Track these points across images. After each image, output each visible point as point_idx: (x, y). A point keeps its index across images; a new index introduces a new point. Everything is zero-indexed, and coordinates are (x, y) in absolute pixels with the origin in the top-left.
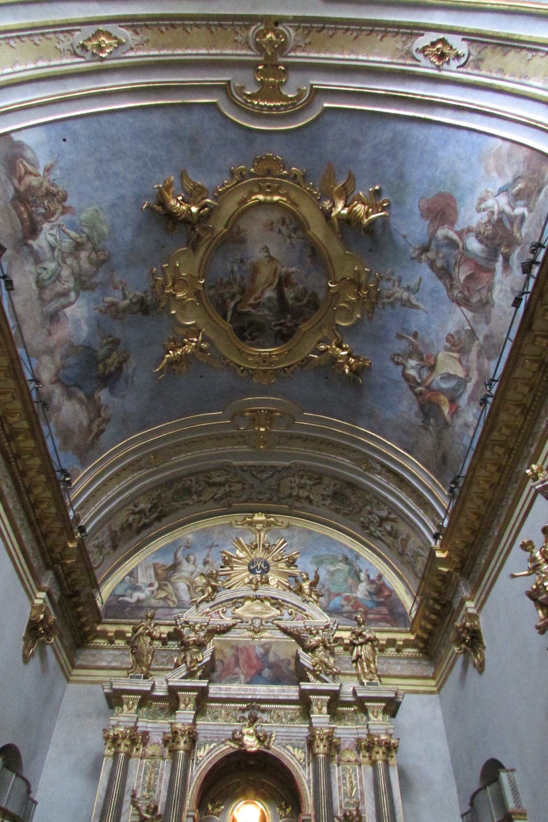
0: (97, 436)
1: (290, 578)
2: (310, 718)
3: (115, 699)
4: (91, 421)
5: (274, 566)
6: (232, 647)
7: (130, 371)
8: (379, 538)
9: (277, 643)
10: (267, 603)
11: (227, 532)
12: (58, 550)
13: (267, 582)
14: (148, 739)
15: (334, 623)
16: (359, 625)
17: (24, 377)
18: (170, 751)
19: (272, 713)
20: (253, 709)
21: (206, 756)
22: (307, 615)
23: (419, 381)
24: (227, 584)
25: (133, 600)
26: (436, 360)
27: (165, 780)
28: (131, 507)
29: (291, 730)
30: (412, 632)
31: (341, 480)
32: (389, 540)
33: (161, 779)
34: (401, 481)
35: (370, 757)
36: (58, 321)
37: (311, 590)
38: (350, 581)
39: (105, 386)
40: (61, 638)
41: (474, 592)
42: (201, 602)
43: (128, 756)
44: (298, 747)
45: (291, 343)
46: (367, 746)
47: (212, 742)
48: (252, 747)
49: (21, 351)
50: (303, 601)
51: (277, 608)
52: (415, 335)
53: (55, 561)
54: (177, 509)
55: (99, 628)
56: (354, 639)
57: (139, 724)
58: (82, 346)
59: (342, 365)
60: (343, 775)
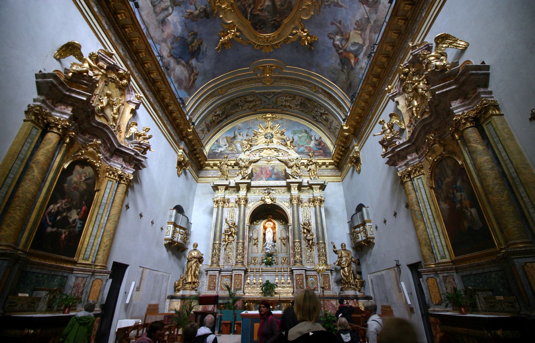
0: (194, 82)
3: (216, 188)
4: (190, 75)
7: (204, 49)
8: (320, 122)
9: (278, 165)
10: (273, 150)
11: (255, 122)
12: (184, 133)
16: (311, 157)
17: (154, 55)
20: (268, 188)
21: (252, 206)
23: (341, 47)
24: (256, 144)
25: (219, 151)
26: (349, 35)
28: (213, 113)
30: (333, 159)
31: (304, 97)
32: (325, 123)
34: (331, 97)
36: (166, 24)
38: (308, 140)
39: (194, 58)
40: (192, 167)
41: (359, 142)
43: (223, 207)
45: (280, 30)
46: (313, 201)
49: (150, 41)
52: (340, 22)
53: (184, 137)
54: (233, 113)
55: (206, 162)
58: (179, 37)
59: (304, 40)
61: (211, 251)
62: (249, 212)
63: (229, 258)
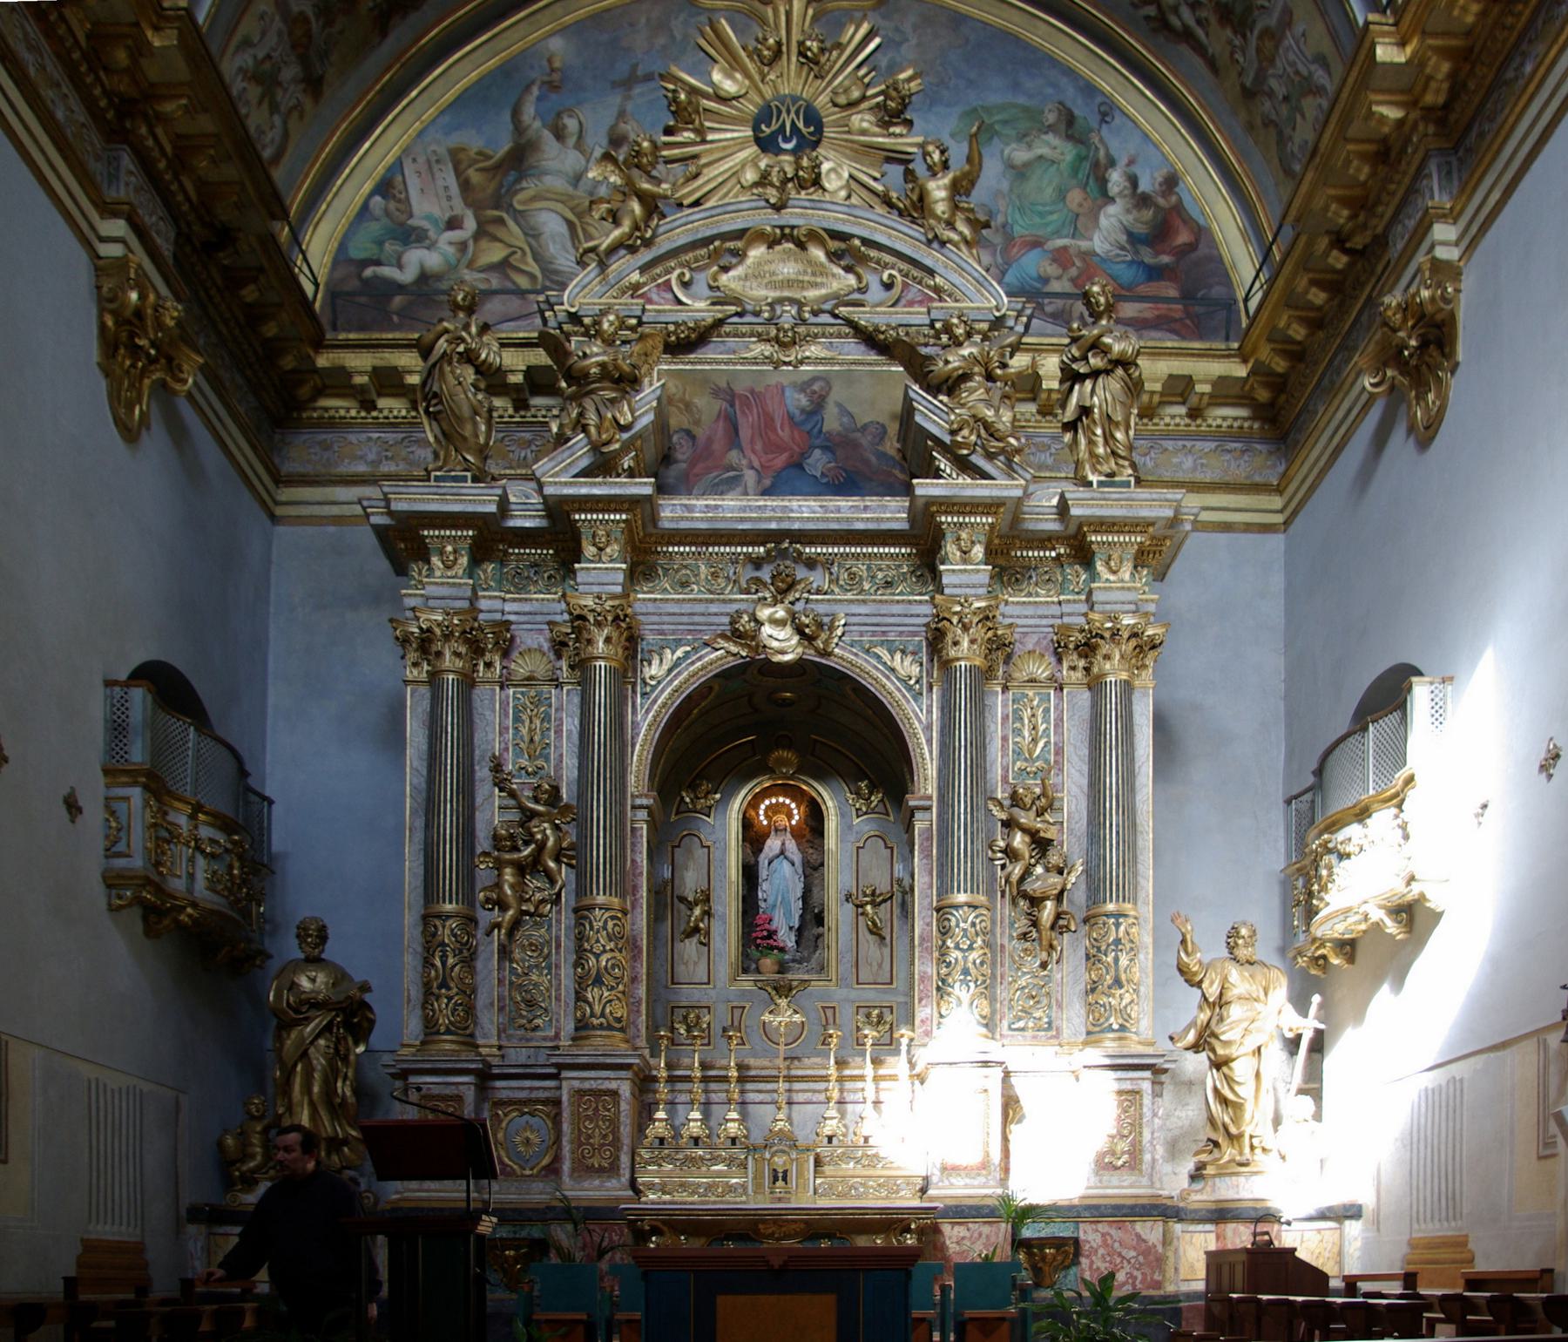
1: (887, 167)
2: (936, 576)
3: (405, 542)
5: (836, 124)
6: (716, 393)
9: (848, 378)
10: (818, 253)
13: (817, 182)
14: (513, 638)
15: (1020, 314)
16: (1096, 316)
18: (572, 667)
19: (835, 569)
20: (780, 556)
21: (669, 675)
22: (937, 290)
24: (688, 192)
27: (570, 732)
29: (884, 609)
33: (559, 732)
35: (1087, 670)
37: (955, 207)
42: (612, 250)
43: (468, 682)
44: (903, 652)
47: (679, 643)
48: (783, 652)
50: (929, 242)
51: (848, 269)
56: (1074, 360)
57: (483, 604)
60: (1015, 711)
61: (410, 962)
62: (645, 722)
63: (531, 1004)
